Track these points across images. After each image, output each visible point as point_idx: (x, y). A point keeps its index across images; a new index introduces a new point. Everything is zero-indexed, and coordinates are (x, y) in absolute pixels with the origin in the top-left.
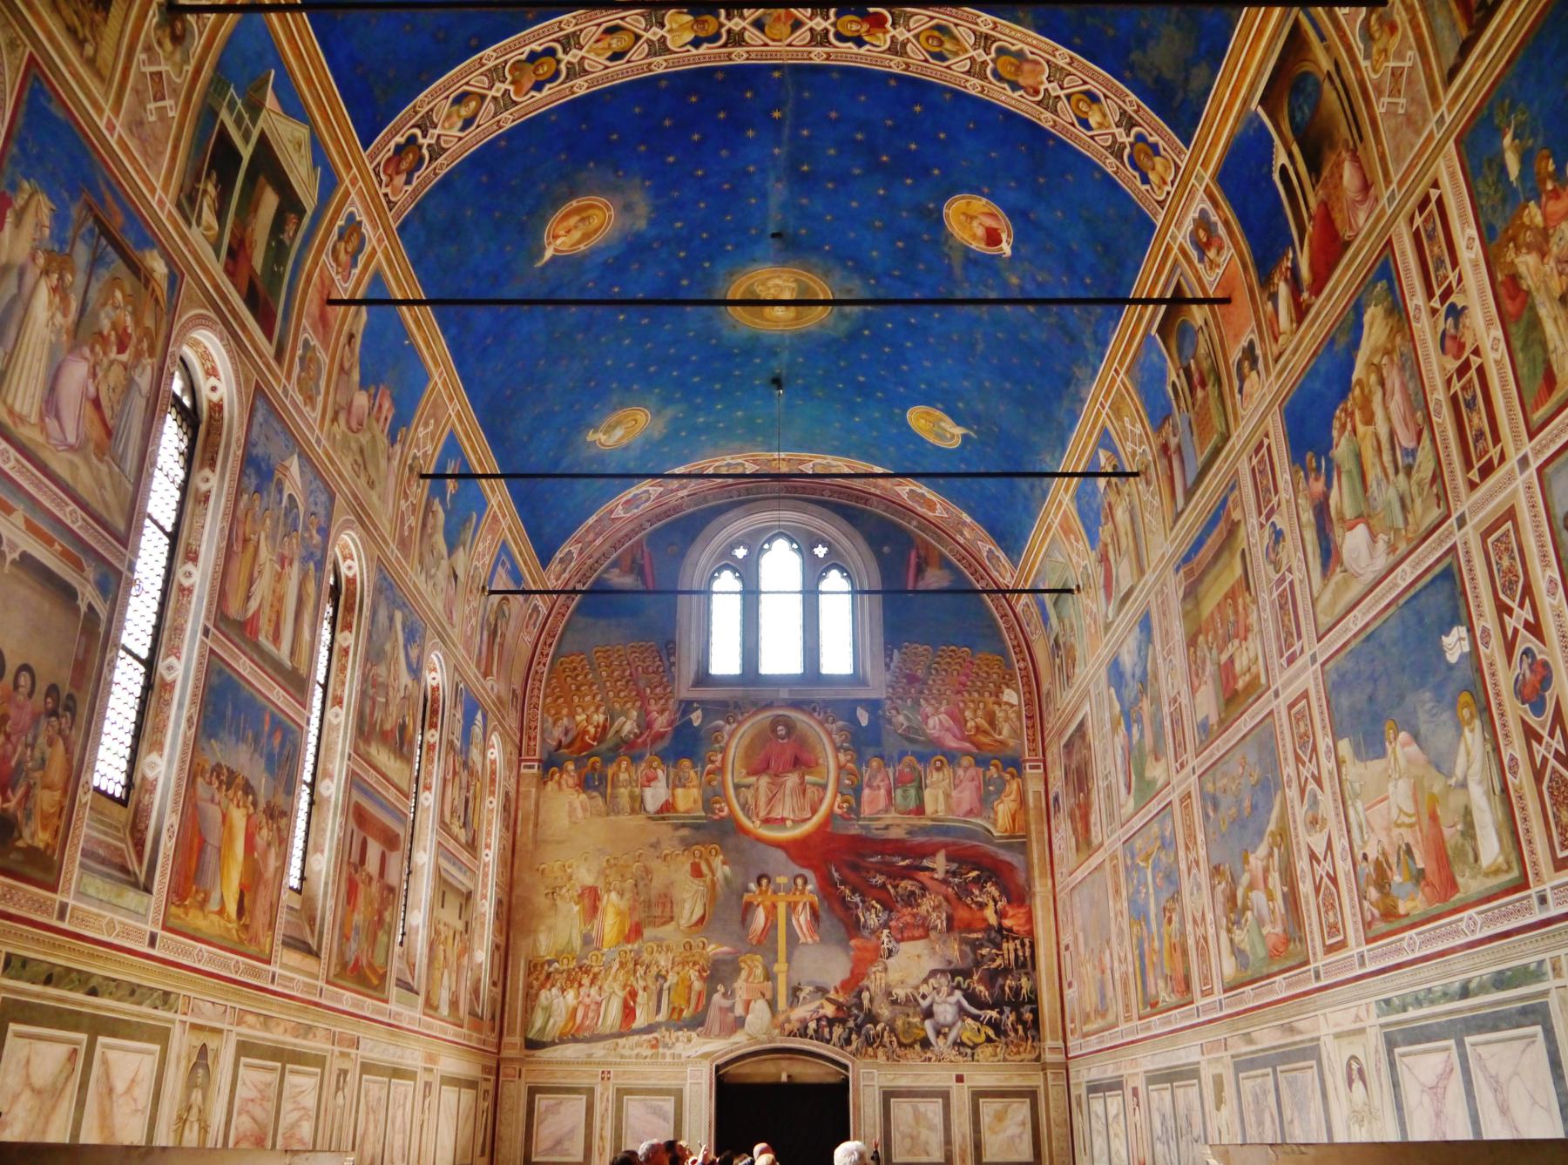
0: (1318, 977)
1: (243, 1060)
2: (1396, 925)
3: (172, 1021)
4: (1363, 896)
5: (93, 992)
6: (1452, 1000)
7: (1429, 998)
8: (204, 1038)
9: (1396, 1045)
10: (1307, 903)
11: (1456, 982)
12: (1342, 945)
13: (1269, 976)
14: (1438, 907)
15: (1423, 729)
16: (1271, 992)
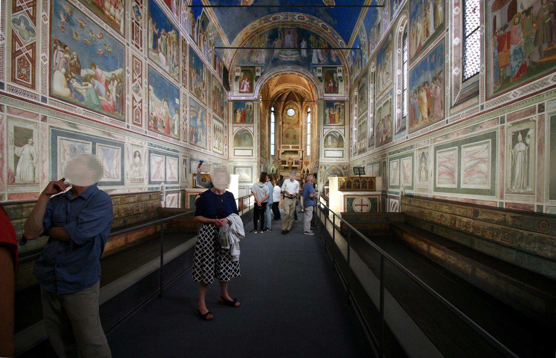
0: (128, 127)
1: (437, 151)
2: (157, 131)
3: (414, 151)
4: (149, 120)
5: (399, 152)
6: (166, 149)
7: (161, 147)
8: (422, 151)
9: (152, 153)
10: (128, 107)
11: (167, 147)
12: (141, 126)
13: (104, 114)
14: (166, 134)
15: (170, 106)
16: (100, 118)
